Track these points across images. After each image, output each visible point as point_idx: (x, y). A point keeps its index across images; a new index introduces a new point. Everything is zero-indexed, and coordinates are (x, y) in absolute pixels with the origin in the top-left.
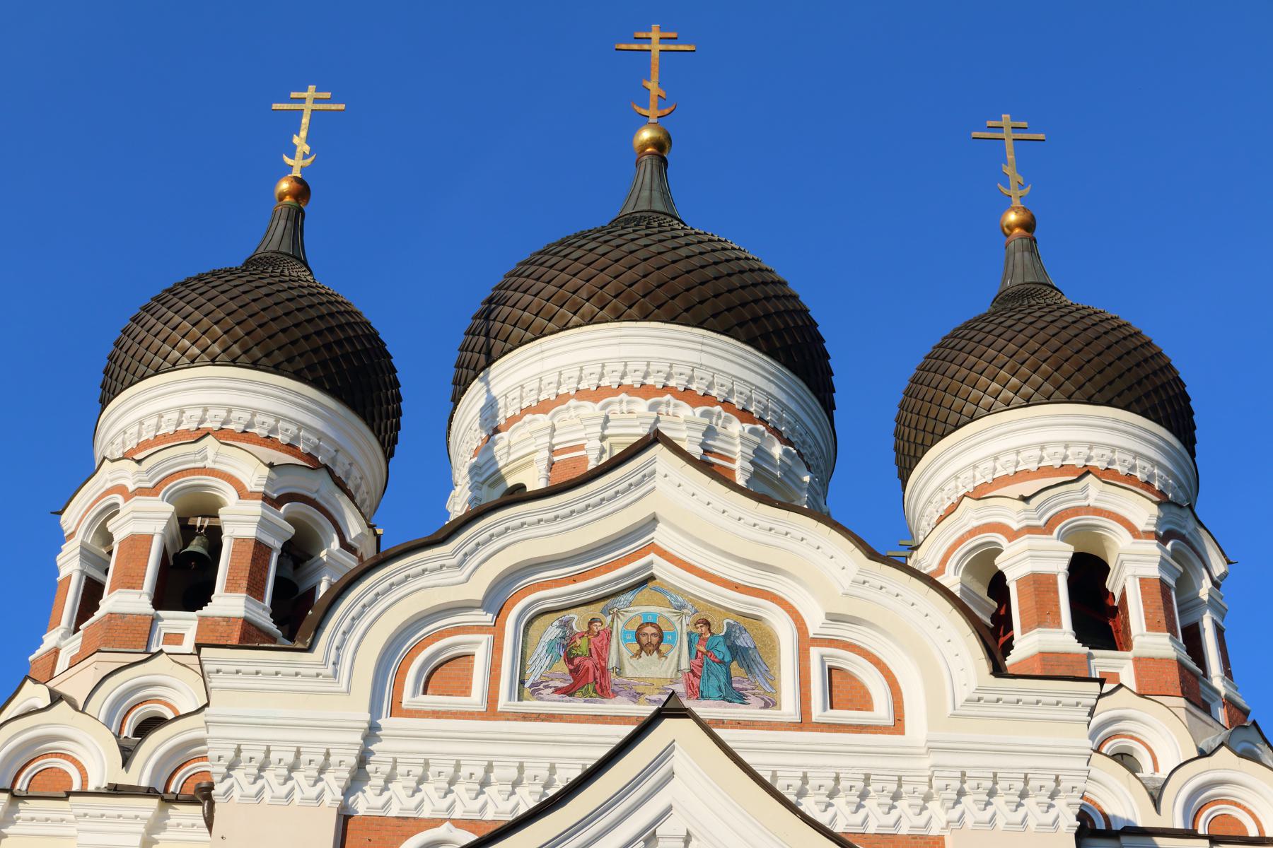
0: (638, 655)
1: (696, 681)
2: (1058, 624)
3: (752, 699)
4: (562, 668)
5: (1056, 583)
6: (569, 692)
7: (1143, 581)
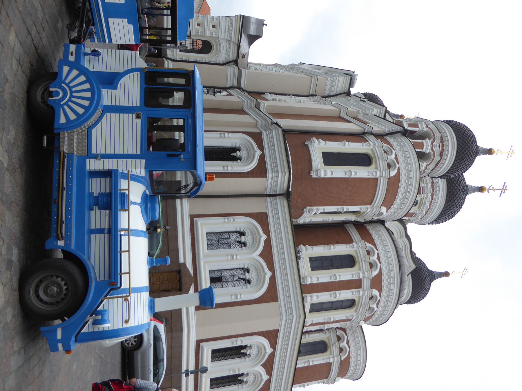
5: (417, 128)
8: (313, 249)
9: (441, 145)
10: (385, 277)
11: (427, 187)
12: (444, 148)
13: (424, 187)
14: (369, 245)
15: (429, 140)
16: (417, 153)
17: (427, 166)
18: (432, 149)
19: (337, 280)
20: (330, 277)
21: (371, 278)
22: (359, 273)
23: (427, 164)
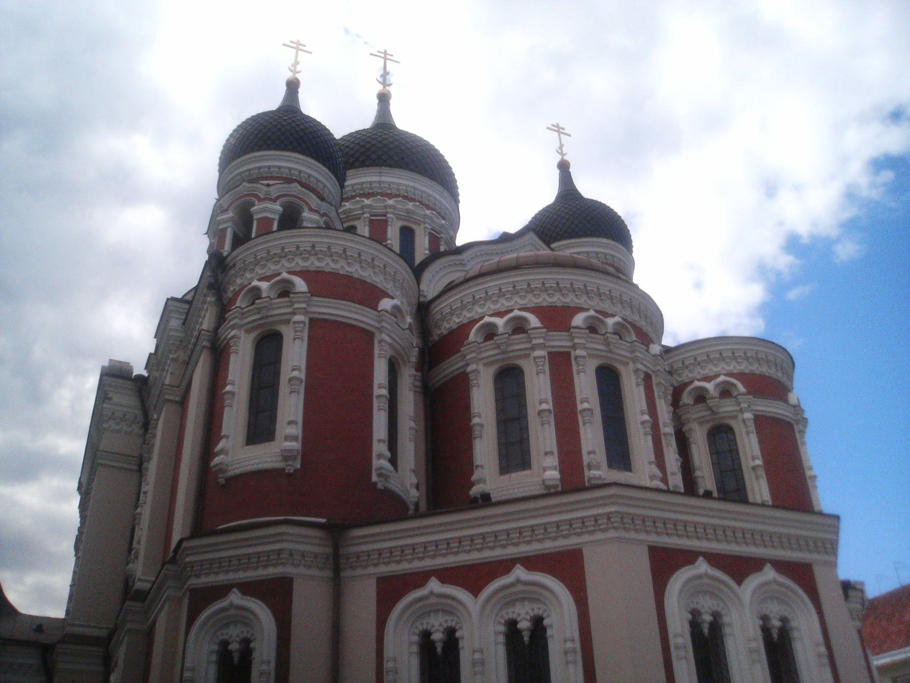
7: (258, 220)
8: (482, 466)
9: (265, 182)
10: (543, 300)
11: (370, 206)
12: (274, 175)
13: (369, 212)
14: (472, 335)
15: (253, 205)
16: (282, 227)
17: (311, 210)
18: (274, 200)
19: (551, 408)
20: (543, 424)
21: (545, 330)
22: (535, 358)
23: (306, 209)
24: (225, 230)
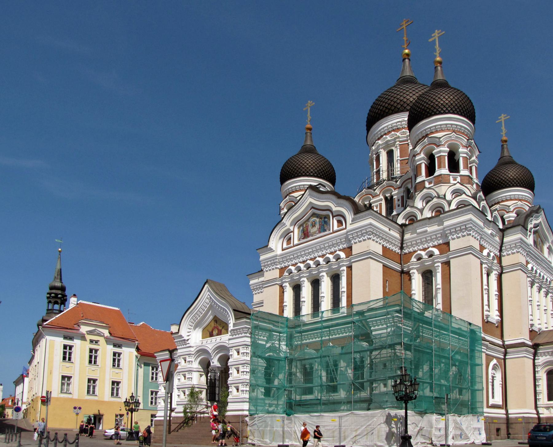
0: (312, 228)
1: (320, 230)
2: (421, 174)
3: (327, 230)
4: (303, 234)
6: (304, 238)
24: (421, 164)
